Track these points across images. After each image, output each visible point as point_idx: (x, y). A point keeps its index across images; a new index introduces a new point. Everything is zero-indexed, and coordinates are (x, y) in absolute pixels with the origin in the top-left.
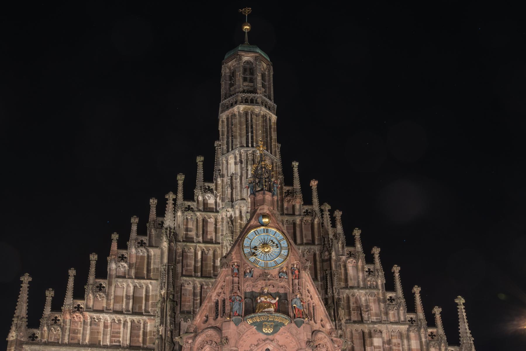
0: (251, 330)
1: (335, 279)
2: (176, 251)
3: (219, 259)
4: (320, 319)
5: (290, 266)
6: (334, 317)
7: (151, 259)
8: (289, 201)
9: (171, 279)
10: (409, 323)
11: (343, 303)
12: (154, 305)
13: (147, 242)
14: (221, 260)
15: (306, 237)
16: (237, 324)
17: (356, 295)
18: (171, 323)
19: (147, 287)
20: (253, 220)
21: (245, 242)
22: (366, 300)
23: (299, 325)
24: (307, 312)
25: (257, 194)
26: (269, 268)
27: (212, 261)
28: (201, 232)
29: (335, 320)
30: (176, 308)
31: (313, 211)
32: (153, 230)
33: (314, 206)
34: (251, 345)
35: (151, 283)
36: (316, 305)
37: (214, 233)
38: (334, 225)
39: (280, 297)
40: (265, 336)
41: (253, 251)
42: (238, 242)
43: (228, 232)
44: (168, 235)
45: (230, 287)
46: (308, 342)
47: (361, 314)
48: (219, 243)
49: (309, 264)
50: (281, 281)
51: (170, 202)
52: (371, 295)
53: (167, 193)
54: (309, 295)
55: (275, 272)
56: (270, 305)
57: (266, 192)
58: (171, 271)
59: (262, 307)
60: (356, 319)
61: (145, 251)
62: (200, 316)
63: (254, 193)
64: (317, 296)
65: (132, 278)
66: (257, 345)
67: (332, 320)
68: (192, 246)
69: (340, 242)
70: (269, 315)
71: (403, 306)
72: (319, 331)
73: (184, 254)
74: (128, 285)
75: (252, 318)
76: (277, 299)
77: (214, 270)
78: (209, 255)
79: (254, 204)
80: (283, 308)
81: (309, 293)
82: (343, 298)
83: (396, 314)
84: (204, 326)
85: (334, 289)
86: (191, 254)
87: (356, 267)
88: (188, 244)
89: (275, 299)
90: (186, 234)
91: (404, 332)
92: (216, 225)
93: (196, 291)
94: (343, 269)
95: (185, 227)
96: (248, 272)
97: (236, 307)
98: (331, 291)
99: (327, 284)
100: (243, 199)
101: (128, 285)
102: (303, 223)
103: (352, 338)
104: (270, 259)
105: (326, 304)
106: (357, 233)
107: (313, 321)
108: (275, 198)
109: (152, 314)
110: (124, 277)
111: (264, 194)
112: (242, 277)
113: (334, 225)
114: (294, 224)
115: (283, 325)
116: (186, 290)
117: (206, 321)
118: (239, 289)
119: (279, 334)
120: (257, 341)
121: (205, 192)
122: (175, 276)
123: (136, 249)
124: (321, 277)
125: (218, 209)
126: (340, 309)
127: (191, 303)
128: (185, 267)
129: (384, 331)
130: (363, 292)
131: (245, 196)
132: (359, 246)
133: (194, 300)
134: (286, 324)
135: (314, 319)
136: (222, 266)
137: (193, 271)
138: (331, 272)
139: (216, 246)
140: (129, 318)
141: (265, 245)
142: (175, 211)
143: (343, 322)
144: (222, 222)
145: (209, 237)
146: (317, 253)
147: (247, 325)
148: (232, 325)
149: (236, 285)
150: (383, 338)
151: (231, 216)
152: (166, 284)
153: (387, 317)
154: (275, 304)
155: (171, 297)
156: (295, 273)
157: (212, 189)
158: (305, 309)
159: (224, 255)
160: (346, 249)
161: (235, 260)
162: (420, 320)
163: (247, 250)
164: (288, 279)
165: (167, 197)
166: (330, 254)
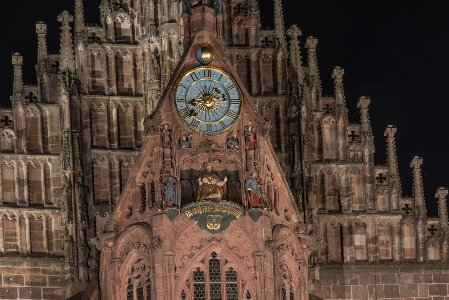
0: (190, 227)
1: (306, 148)
2: (80, 109)
3: (142, 120)
4: (284, 208)
5: (243, 129)
6: (303, 205)
7: (46, 123)
8: (240, 23)
9: (77, 153)
10: (403, 212)
11: (315, 184)
12: (58, 193)
13: (38, 95)
14: (145, 121)
15: (265, 83)
16: (171, 218)
17: (334, 172)
18: (83, 219)
19: (46, 166)
20: (189, 55)
21: (178, 92)
22: (347, 179)
23: (255, 217)
24: (265, 198)
25: (193, 11)
26: (213, 133)
27: (132, 123)
28: (114, 78)
29: (304, 210)
30: (88, 196)
31: (275, 39)
32: (45, 77)
33: (277, 31)
34: (192, 247)
35: (50, 160)
36: (278, 189)
37: (133, 80)
38: (305, 63)
39: (229, 177)
40: (210, 234)
41: (191, 107)
42: (168, 93)
43: (152, 76)
44: (68, 84)
45: (160, 164)
46: (268, 242)
47: (339, 200)
48: (141, 95)
49: (269, 126)
50: (230, 153)
51: (66, 28)
52: (354, 171)
53: (60, 12)
54: (269, 174)
55: (221, 139)
56: (215, 189)
57: (207, 8)
58: (76, 140)
59: (205, 192)
60: (332, 208)
61: (36, 109)
62: (121, 207)
63: (188, 11)
64: (279, 175)
65: (22, 153)
66: (199, 248)
67: (300, 210)
68: (103, 100)
69: (314, 90)
70: (214, 204)
71: (396, 188)
72: (282, 226)
73: (93, 113)
74: (19, 164)
75: (191, 208)
76: (226, 180)
77: (136, 138)
78: (127, 115)
79: (190, 29)
80: (233, 194)
81: (269, 170)
82: (316, 176)
83: (387, 200)
84: (127, 222)
85: (304, 164)
86: (103, 114)
87: (335, 129)
88: (97, 97)
89: (223, 180)
90: (94, 82)
91: (396, 226)
92: (135, 65)
93: (113, 171)
94: (316, 132)
95: (90, 69)
96: (184, 139)
97: (170, 194)
98: (299, 166)
99: (294, 157)
100: (172, 21)
101: (19, 164)
102: (261, 60)
103: (326, 235)
104: (214, 119)
105: (292, 186)
106: (338, 74)
107: (274, 212)
108: (220, 17)
109: (56, 205)
110: (11, 152)
111: (203, 11)
112: (175, 147)
113: (305, 63)
114: (248, 61)
115: (234, 218)
116: (99, 169)
117: (130, 215)
118: (172, 167)
119: (228, 232)
120: (200, 242)
121: (116, 10)
122: (83, 149)
123: (24, 107)
124: (285, 146)
125: (136, 38)
126: (311, 193)
127: (108, 189)
128: (96, 134)
129: (370, 225)
130: (343, 167)
131: (174, 15)
132: (340, 95)
133: (111, 183)
134: (238, 217)
135: (276, 209)
136: (147, 130)
137: (107, 139)
138: (300, 137)
139: (137, 99)
140: (25, 213)
141: (207, 96)
142: (74, 44)
143: (315, 212)
144: (144, 60)
145: (126, 85)
146: (281, 107)
147: (186, 220)
148: (166, 220)
149: (168, 160)
150: (367, 234)
151: (156, 51)
152: (71, 161)
153: (374, 205)
154: (222, 187)
155: (80, 180)
156: (249, 140)
157: (126, 4)
158: (263, 195)
159: (149, 113)
160: (321, 101)
161: (165, 122)
162: (418, 207)
163: (181, 106)
164: (240, 149)
165: (60, 19)
166: (299, 109)
